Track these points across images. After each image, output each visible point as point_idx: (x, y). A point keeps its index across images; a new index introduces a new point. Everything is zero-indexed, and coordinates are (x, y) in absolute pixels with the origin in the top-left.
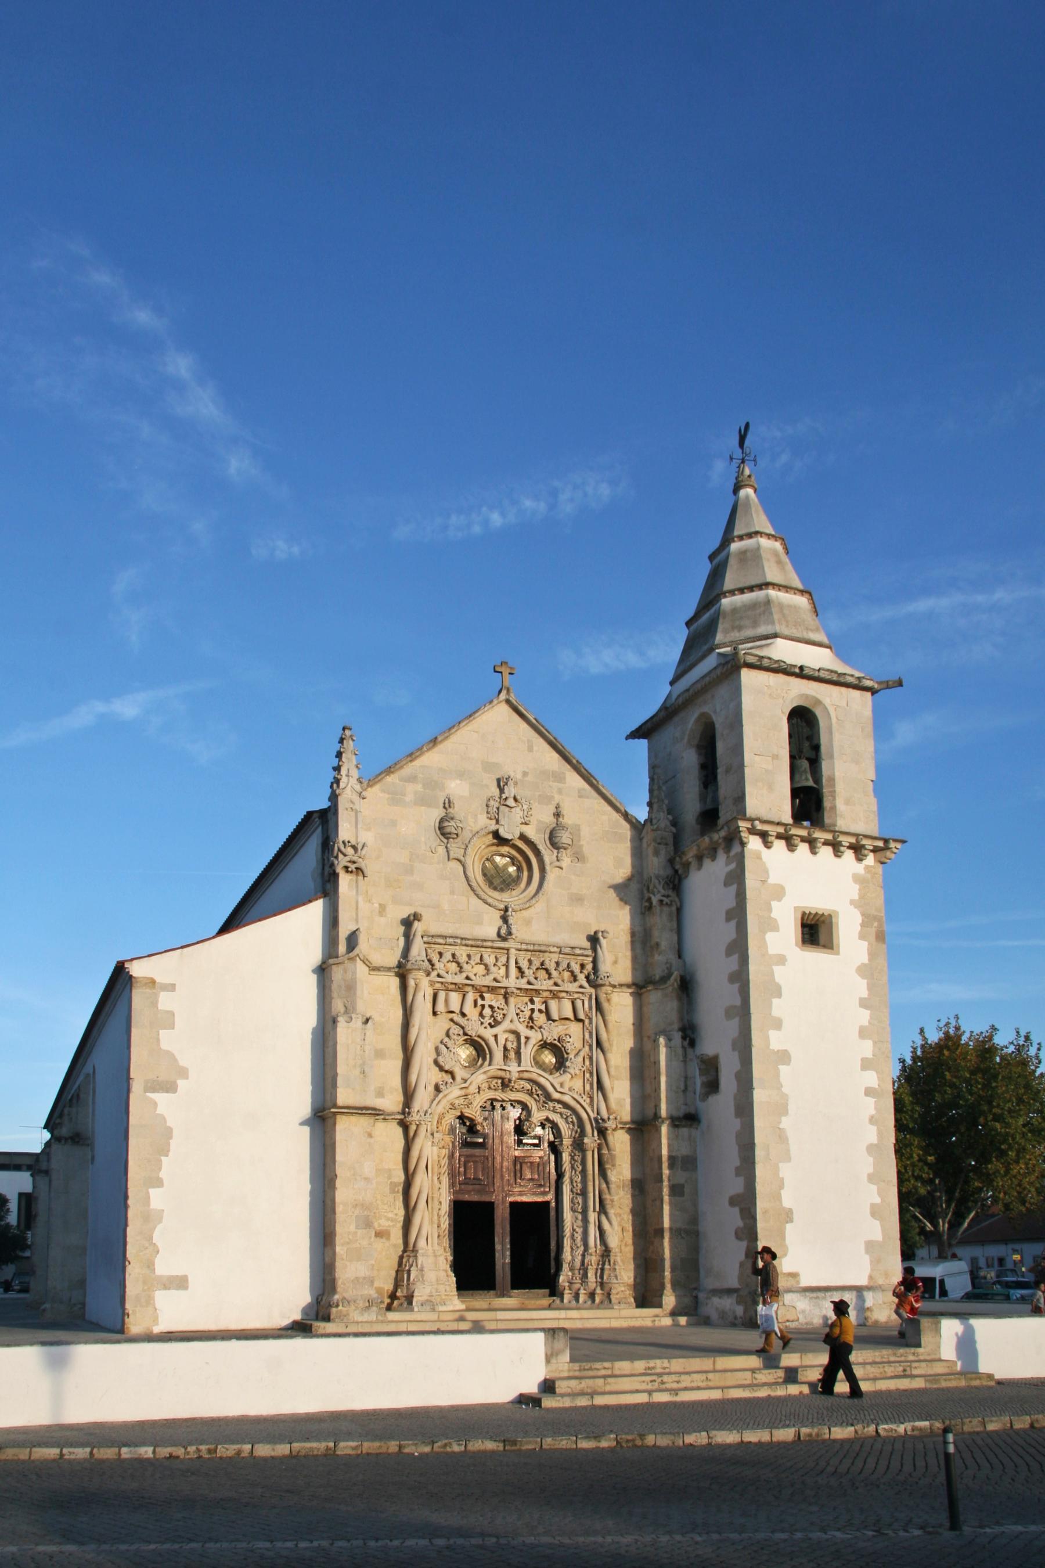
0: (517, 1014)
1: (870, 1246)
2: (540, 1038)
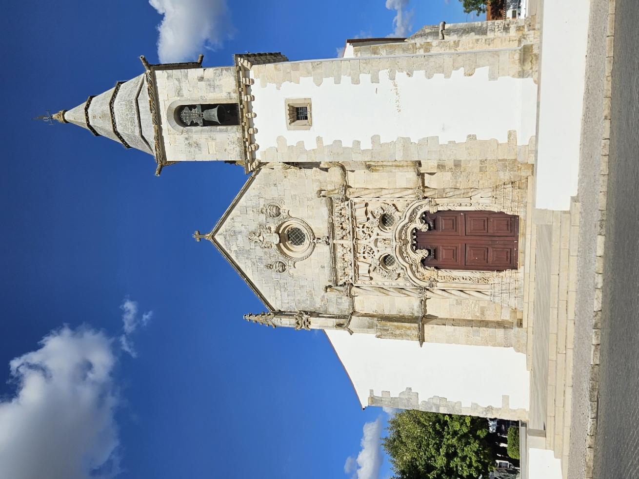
0: (366, 239)
1: (492, 77)
2: (377, 228)
